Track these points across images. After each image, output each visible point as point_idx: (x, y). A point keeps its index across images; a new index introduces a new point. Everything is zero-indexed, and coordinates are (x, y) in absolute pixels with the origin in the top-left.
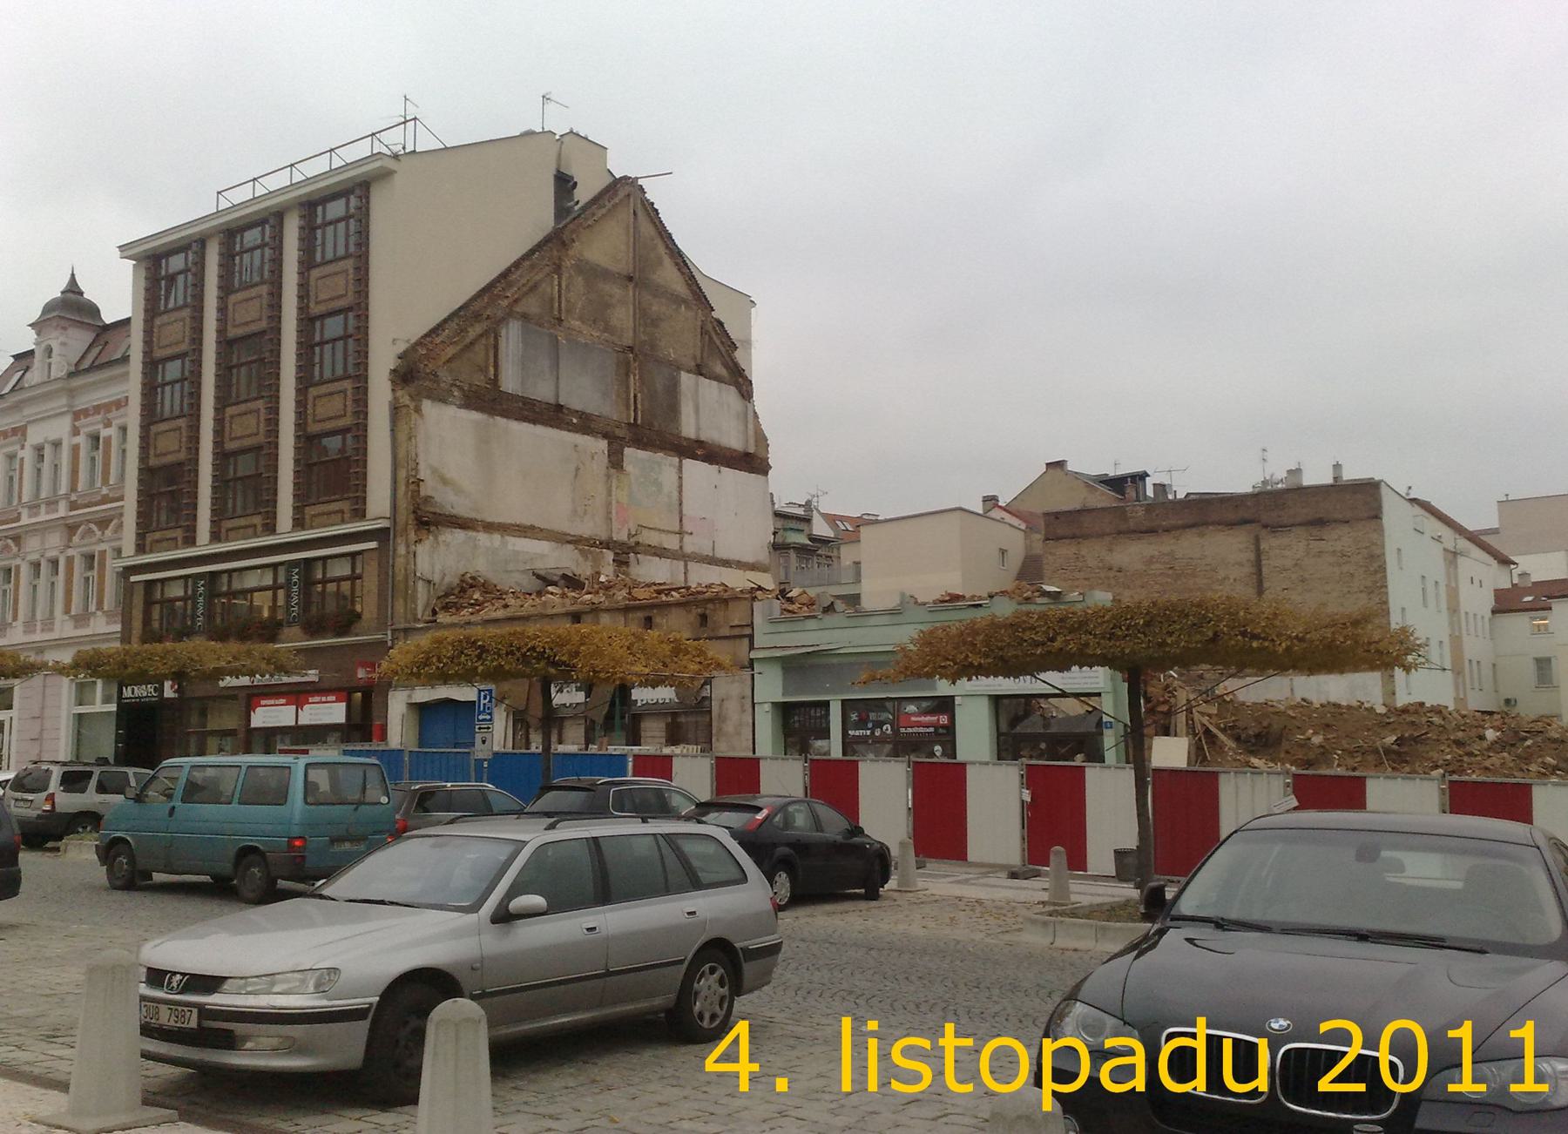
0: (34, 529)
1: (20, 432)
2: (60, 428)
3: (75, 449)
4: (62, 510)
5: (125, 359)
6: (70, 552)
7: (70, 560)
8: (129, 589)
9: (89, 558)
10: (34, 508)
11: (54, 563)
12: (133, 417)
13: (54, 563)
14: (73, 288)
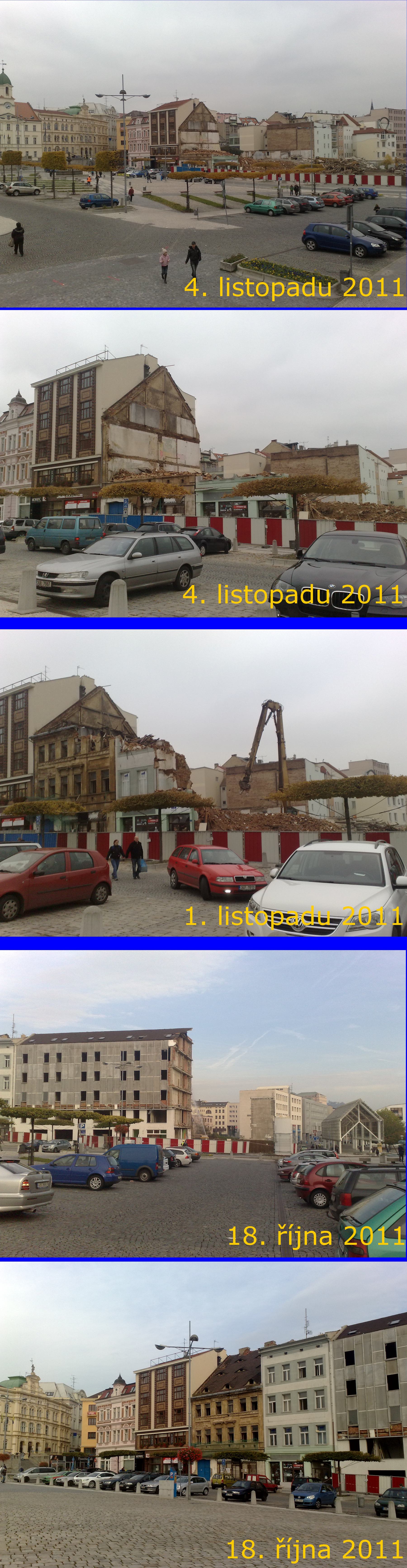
0: (114, 1424)
1: (111, 1405)
2: (120, 1405)
3: (123, 1409)
4: (120, 1421)
5: (135, 1392)
9: (126, 1430)
10: (114, 1420)
11: (119, 1431)
12: (137, 1404)
13: (119, 1431)
14: (120, 1377)
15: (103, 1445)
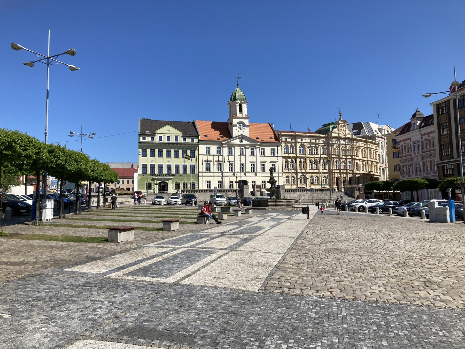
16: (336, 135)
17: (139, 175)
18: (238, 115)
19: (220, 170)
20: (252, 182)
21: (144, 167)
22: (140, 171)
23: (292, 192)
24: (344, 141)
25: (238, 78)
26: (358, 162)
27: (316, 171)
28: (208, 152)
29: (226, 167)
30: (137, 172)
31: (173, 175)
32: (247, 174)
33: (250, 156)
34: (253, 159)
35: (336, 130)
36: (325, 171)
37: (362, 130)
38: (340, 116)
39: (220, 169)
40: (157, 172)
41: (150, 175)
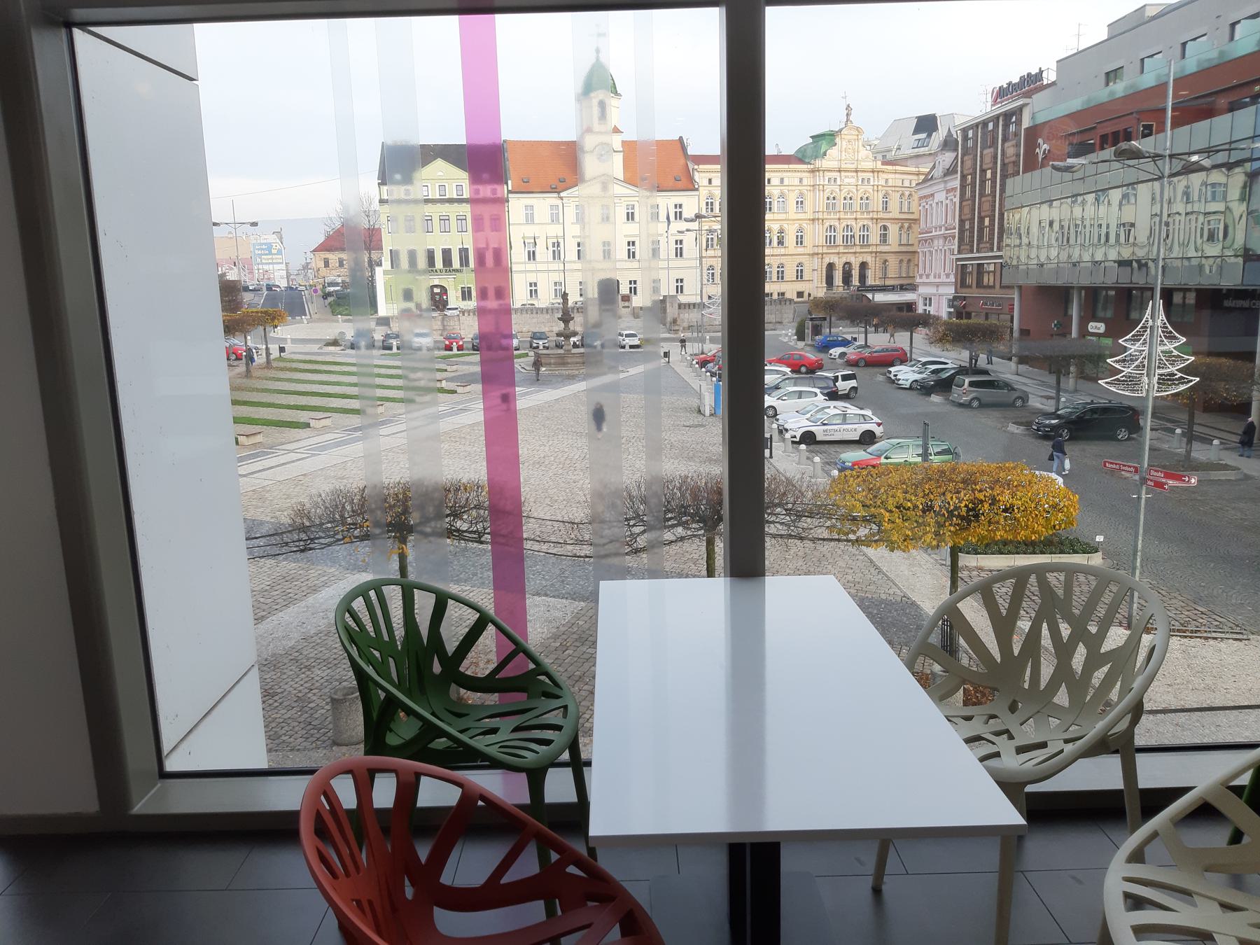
1: (932, 195)
6: (945, 248)
7: (945, 250)
8: (957, 265)
13: (941, 250)
15: (924, 280)
16: (835, 165)
17: (385, 272)
18: (597, 126)
19: (560, 259)
20: (630, 282)
21: (394, 255)
22: (386, 264)
23: (695, 310)
24: (853, 177)
25: (599, 35)
26: (888, 224)
27: (782, 251)
28: (530, 219)
29: (570, 252)
30: (380, 264)
31: (457, 271)
32: (619, 265)
33: (624, 223)
34: (631, 229)
35: (833, 152)
36: (801, 250)
37: (934, 134)
38: (847, 115)
39: (556, 255)
40: (422, 263)
41: (409, 272)
